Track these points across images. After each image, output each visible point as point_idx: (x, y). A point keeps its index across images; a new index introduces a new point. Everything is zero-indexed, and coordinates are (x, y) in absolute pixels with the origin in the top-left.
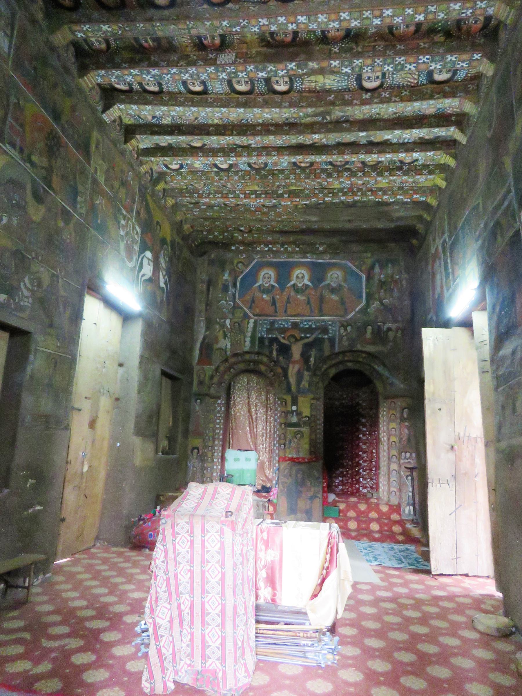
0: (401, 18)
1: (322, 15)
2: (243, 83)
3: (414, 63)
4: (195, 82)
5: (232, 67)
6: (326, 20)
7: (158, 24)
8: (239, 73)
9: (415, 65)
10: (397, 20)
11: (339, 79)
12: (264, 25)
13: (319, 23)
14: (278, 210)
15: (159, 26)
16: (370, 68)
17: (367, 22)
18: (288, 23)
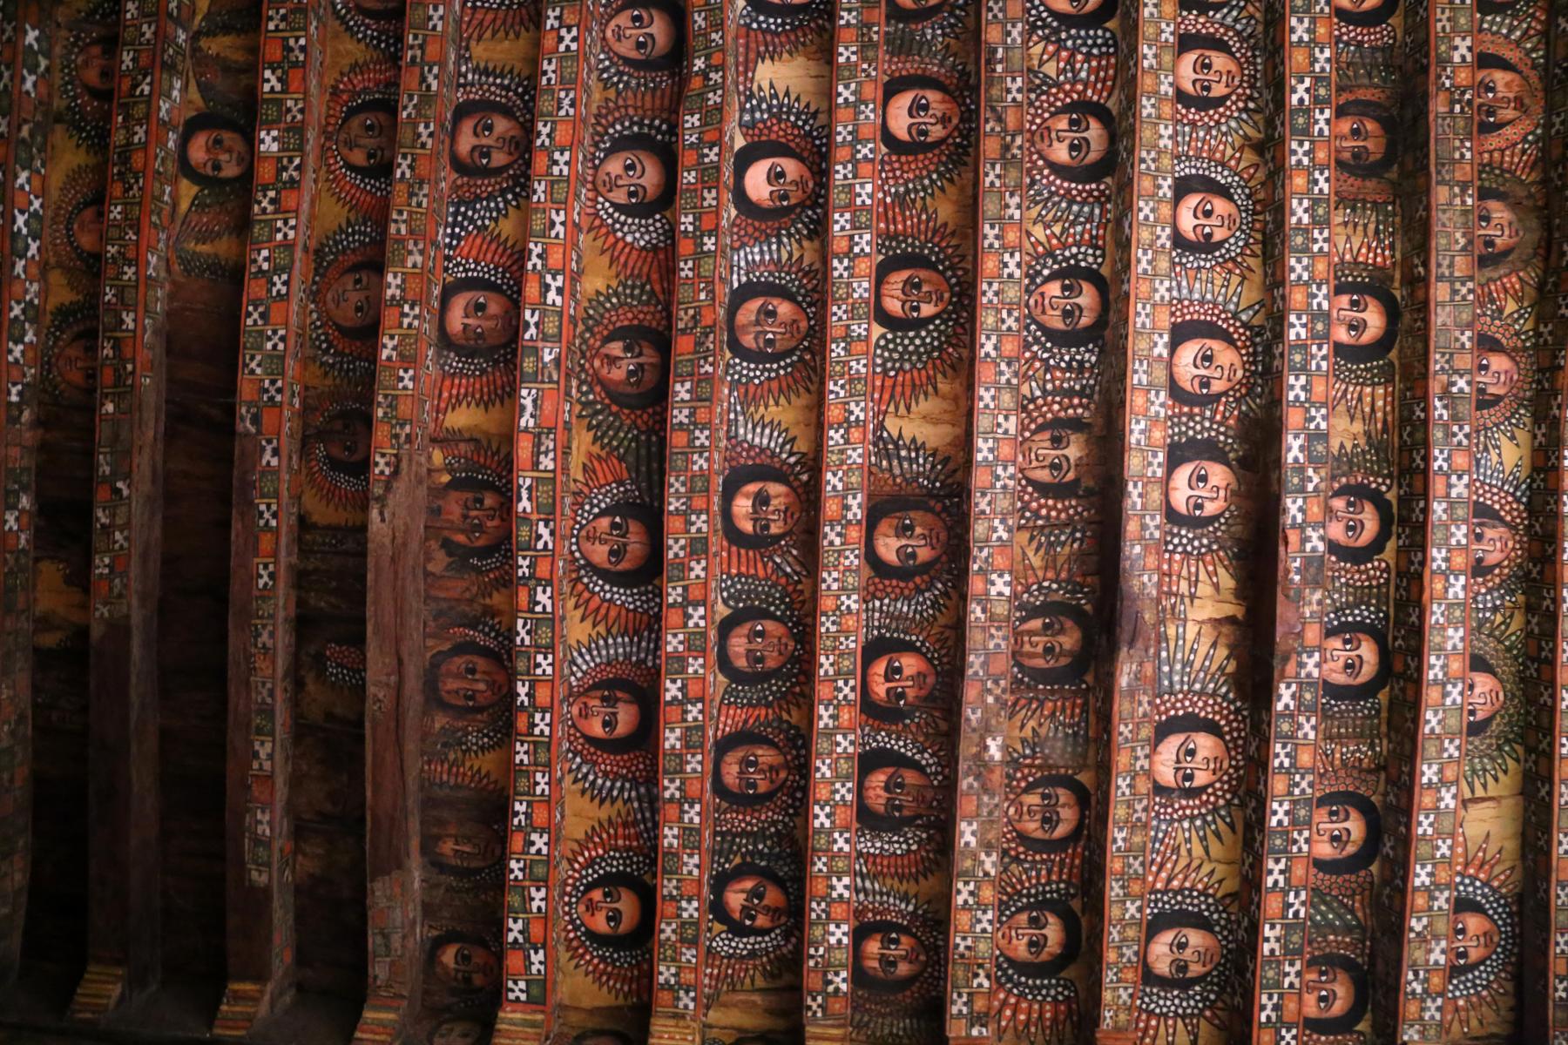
0: (1430, 831)
1: (1462, 639)
2: (1202, 372)
3: (1287, 880)
4: (1214, 221)
5: (1324, 365)
6: (1449, 646)
7: (1469, 201)
8: (1303, 379)
9: (1281, 884)
10: (1426, 823)
11: (1197, 665)
12: (1450, 486)
13: (1444, 629)
14: (430, 353)
15: (1463, 202)
16: (1287, 763)
17: (1431, 749)
18: (1449, 551)
